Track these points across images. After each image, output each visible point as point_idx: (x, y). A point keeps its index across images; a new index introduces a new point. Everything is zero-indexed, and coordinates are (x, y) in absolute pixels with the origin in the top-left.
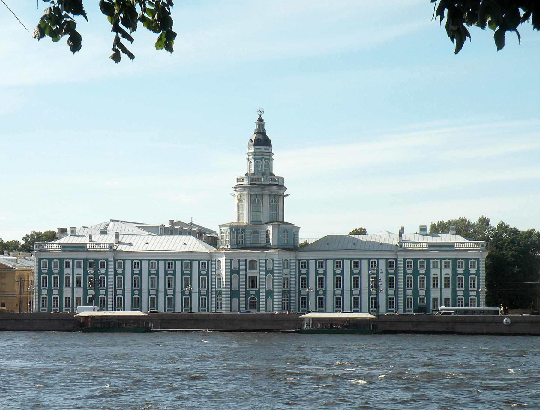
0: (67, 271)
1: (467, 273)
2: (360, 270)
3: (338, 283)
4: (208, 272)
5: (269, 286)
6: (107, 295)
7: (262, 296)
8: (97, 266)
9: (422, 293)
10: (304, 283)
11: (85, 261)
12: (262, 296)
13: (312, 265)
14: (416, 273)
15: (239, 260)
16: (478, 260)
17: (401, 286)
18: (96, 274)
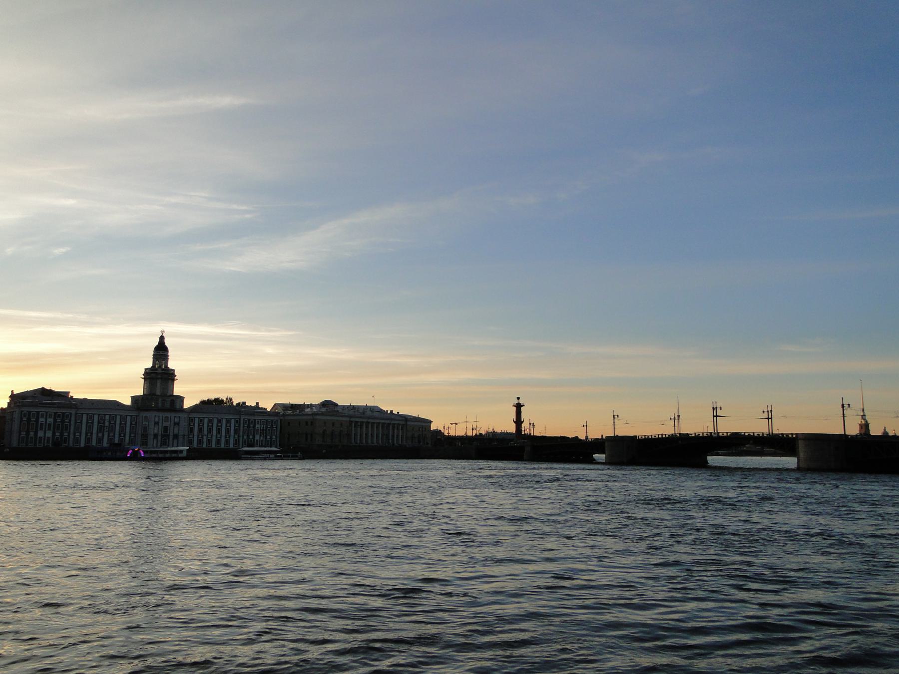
0: (41, 420)
1: (272, 427)
2: (222, 425)
3: (210, 431)
4: (136, 423)
5: (176, 431)
6: (69, 436)
7: (171, 439)
8: (63, 416)
9: (251, 437)
10: (191, 430)
11: (55, 413)
12: (171, 439)
13: (197, 421)
14: (249, 426)
15: (159, 416)
16: (277, 420)
17: (241, 434)
18: (63, 421)
